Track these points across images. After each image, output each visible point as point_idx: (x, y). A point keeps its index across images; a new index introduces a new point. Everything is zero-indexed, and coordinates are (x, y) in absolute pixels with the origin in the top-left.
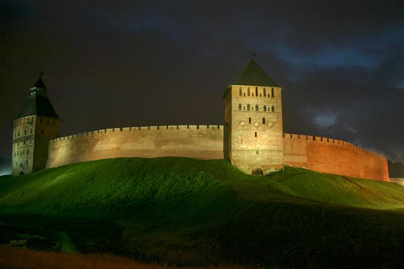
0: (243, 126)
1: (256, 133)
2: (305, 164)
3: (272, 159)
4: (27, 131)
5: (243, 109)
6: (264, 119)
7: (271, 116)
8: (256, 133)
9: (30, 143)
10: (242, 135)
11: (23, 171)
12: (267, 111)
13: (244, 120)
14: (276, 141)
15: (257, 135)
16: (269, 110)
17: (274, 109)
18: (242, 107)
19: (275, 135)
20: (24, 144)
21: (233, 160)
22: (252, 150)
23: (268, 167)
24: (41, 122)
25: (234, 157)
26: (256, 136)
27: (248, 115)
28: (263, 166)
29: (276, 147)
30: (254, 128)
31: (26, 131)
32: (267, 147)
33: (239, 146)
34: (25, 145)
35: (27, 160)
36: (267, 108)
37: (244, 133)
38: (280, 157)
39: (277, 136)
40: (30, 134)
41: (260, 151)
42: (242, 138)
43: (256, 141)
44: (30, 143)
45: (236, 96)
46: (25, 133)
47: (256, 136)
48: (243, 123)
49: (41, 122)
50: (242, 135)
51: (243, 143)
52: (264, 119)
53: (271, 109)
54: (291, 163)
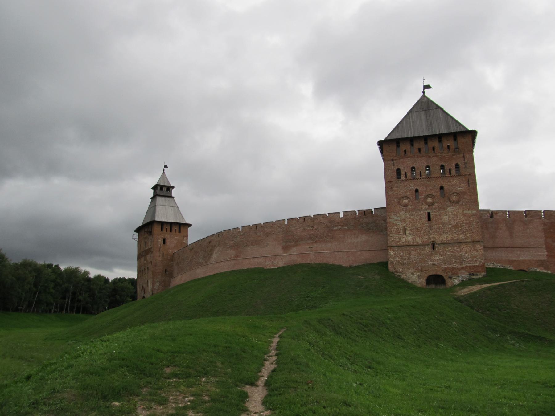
0: (406, 206)
1: (429, 214)
2: (541, 263)
3: (461, 257)
4: (147, 242)
5: (403, 178)
6: (442, 188)
7: (454, 182)
8: (429, 214)
9: (150, 259)
10: (403, 221)
11: (145, 296)
12: (447, 174)
13: (407, 194)
14: (466, 224)
15: (431, 217)
16: (450, 174)
17: (462, 170)
18: (403, 173)
19: (464, 215)
20: (145, 260)
21: (392, 263)
22: (424, 245)
23: (454, 272)
24: (162, 230)
25: (393, 258)
26: (429, 219)
27: (412, 186)
28: (445, 270)
29: (468, 235)
30: (425, 206)
31: (146, 242)
32: (450, 237)
33: (400, 239)
34: (145, 262)
35: (147, 281)
36: (447, 169)
37: (408, 215)
38: (477, 251)
39: (468, 216)
40: (150, 247)
41: (439, 244)
42: (404, 225)
43: (430, 227)
44: (150, 259)
45: (391, 158)
46: (146, 247)
47: (429, 219)
48: (405, 201)
49: (162, 230)
50: (403, 221)
51: (407, 232)
52: (442, 188)
53: (453, 171)
54: (511, 262)
